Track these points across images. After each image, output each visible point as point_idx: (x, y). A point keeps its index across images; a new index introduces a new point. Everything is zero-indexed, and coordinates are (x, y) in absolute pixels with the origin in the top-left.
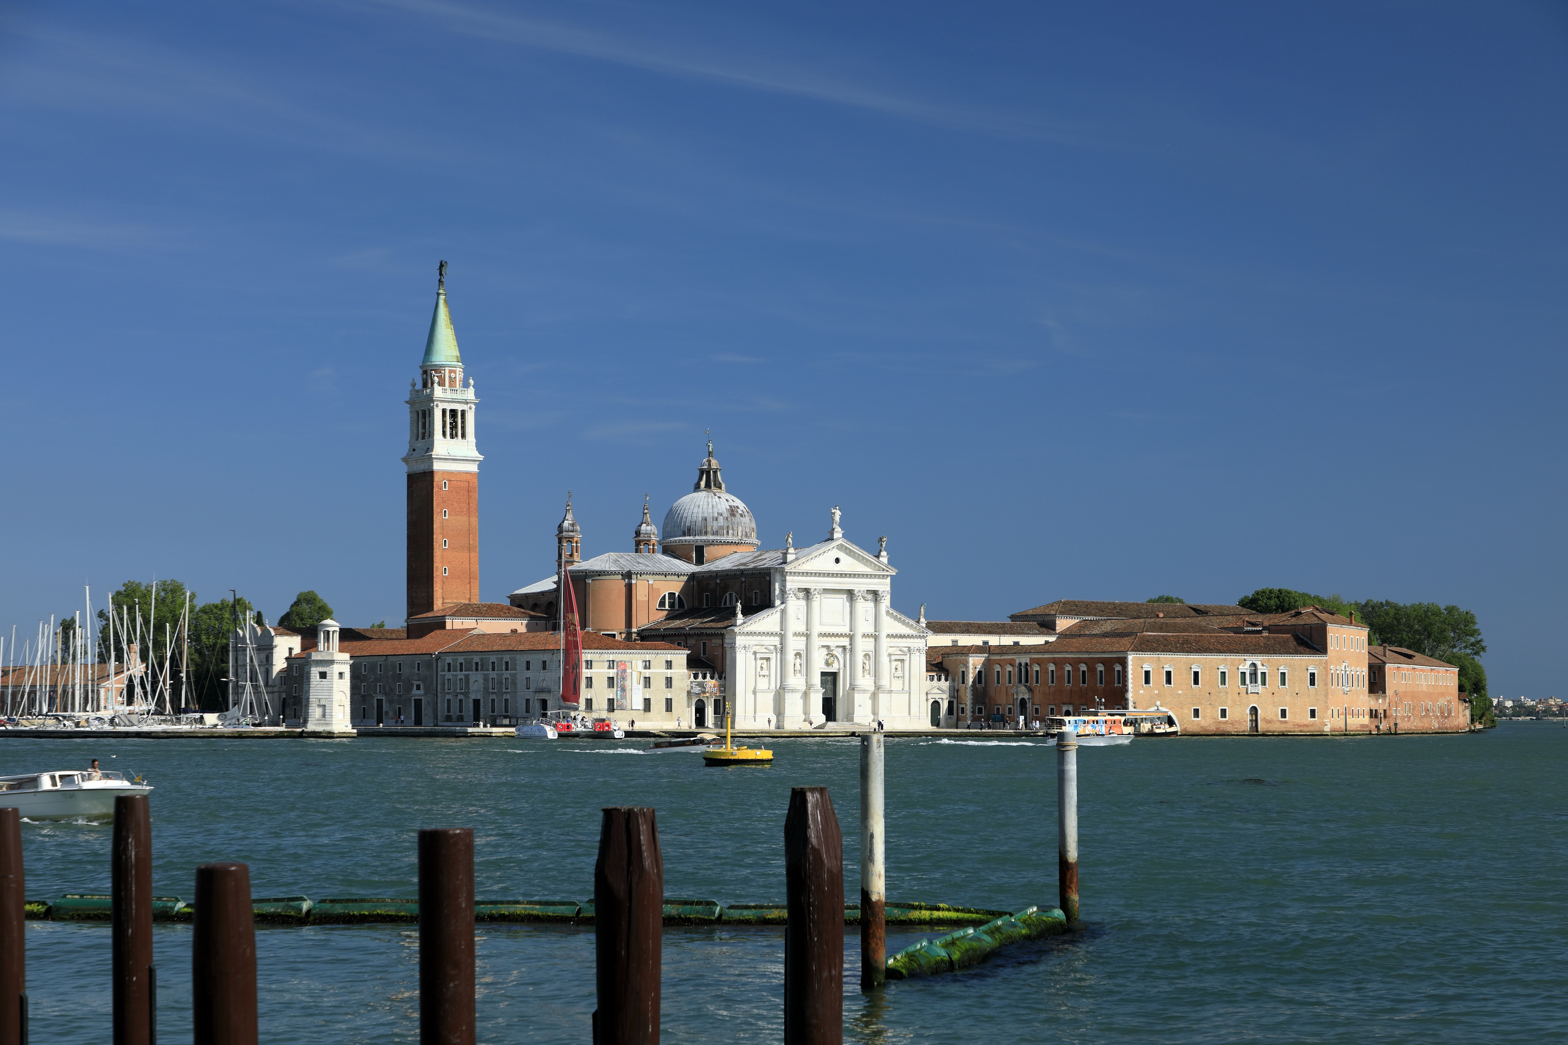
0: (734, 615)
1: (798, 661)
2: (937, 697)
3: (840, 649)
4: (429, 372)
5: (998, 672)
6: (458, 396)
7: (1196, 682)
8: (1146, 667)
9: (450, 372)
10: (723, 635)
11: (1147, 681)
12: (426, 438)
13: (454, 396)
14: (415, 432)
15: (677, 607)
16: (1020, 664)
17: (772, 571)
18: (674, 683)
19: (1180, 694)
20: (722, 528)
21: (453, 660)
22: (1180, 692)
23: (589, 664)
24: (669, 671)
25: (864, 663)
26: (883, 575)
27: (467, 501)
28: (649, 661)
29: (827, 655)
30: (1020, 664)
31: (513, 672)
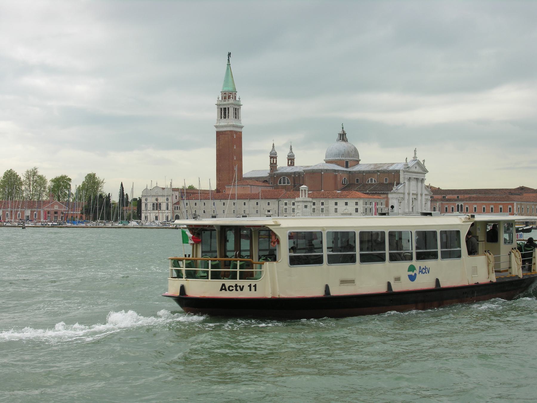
0: (393, 185)
3: (414, 200)
4: (227, 94)
5: (446, 208)
6: (237, 103)
10: (387, 194)
12: (227, 118)
14: (220, 116)
15: (346, 183)
16: (458, 205)
17: (401, 171)
20: (354, 155)
21: (288, 201)
28: (378, 203)
30: (458, 205)
31: (327, 206)
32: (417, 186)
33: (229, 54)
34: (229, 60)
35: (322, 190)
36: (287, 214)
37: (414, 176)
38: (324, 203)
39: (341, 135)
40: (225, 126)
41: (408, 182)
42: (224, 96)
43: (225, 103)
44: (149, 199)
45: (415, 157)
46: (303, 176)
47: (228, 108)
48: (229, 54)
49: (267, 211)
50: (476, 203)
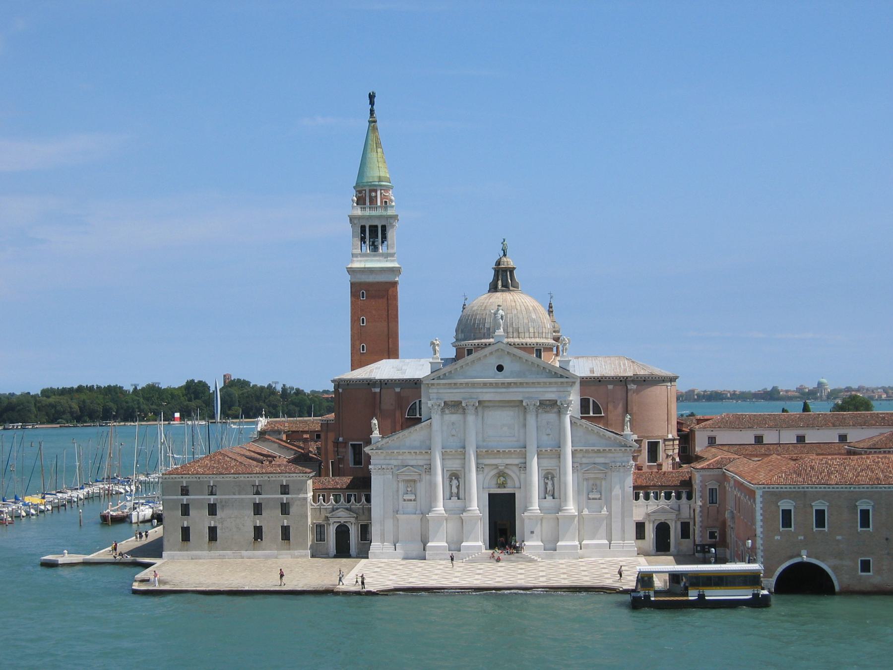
1: (455, 482)
2: (662, 518)
3: (515, 469)
7: (865, 522)
8: (785, 504)
9: (371, 191)
11: (787, 522)
13: (374, 213)
18: (293, 510)
19: (838, 541)
22: (839, 538)
23: (185, 491)
24: (285, 497)
25: (546, 484)
26: (562, 383)
27: (386, 308)
29: (495, 475)
32: (525, 426)
33: (372, 97)
34: (372, 112)
35: (340, 438)
37: (488, 395)
41: (455, 418)
48: (372, 97)
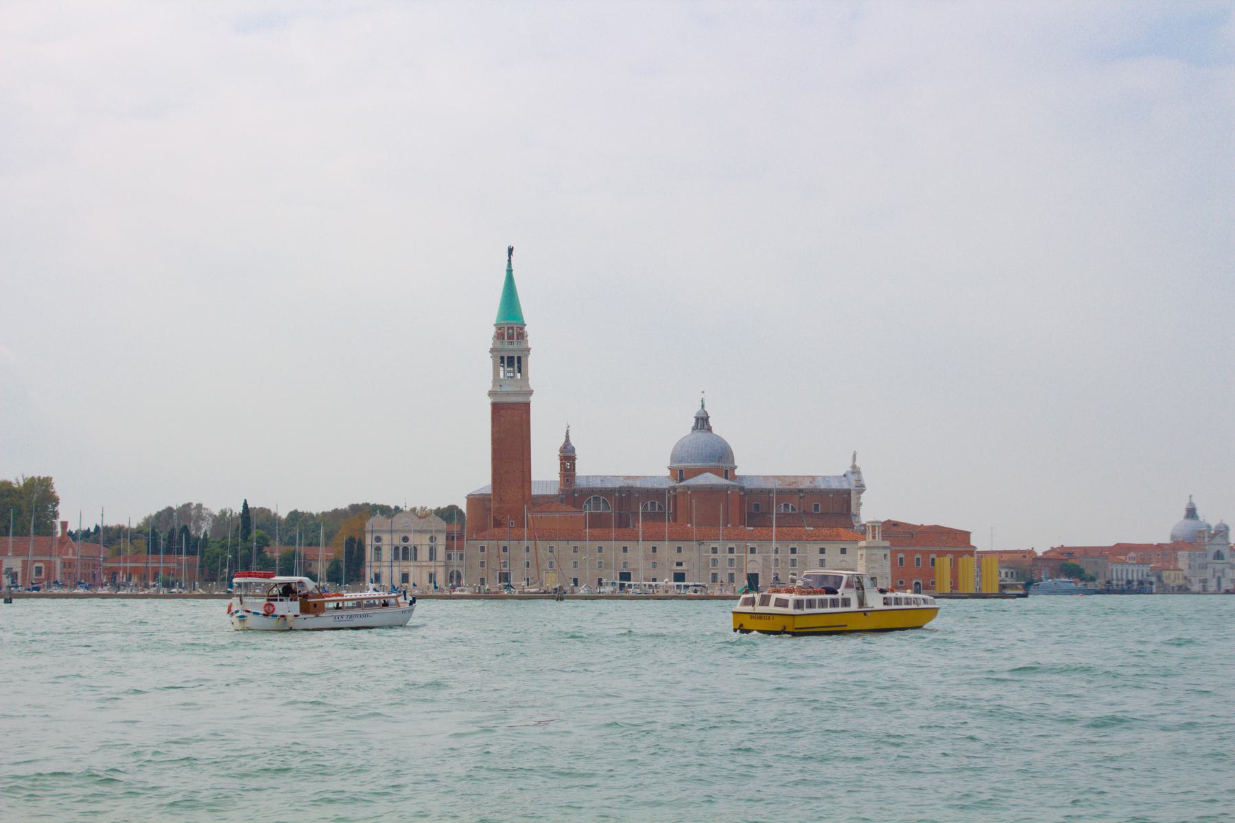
4: (515, 328)
33: (511, 251)
34: (510, 261)
36: (718, 569)
38: (797, 548)
39: (702, 419)
40: (515, 394)
42: (508, 334)
43: (511, 347)
44: (386, 538)
45: (854, 467)
46: (637, 495)
47: (519, 358)
48: (511, 251)
49: (675, 564)
50: (903, 550)
